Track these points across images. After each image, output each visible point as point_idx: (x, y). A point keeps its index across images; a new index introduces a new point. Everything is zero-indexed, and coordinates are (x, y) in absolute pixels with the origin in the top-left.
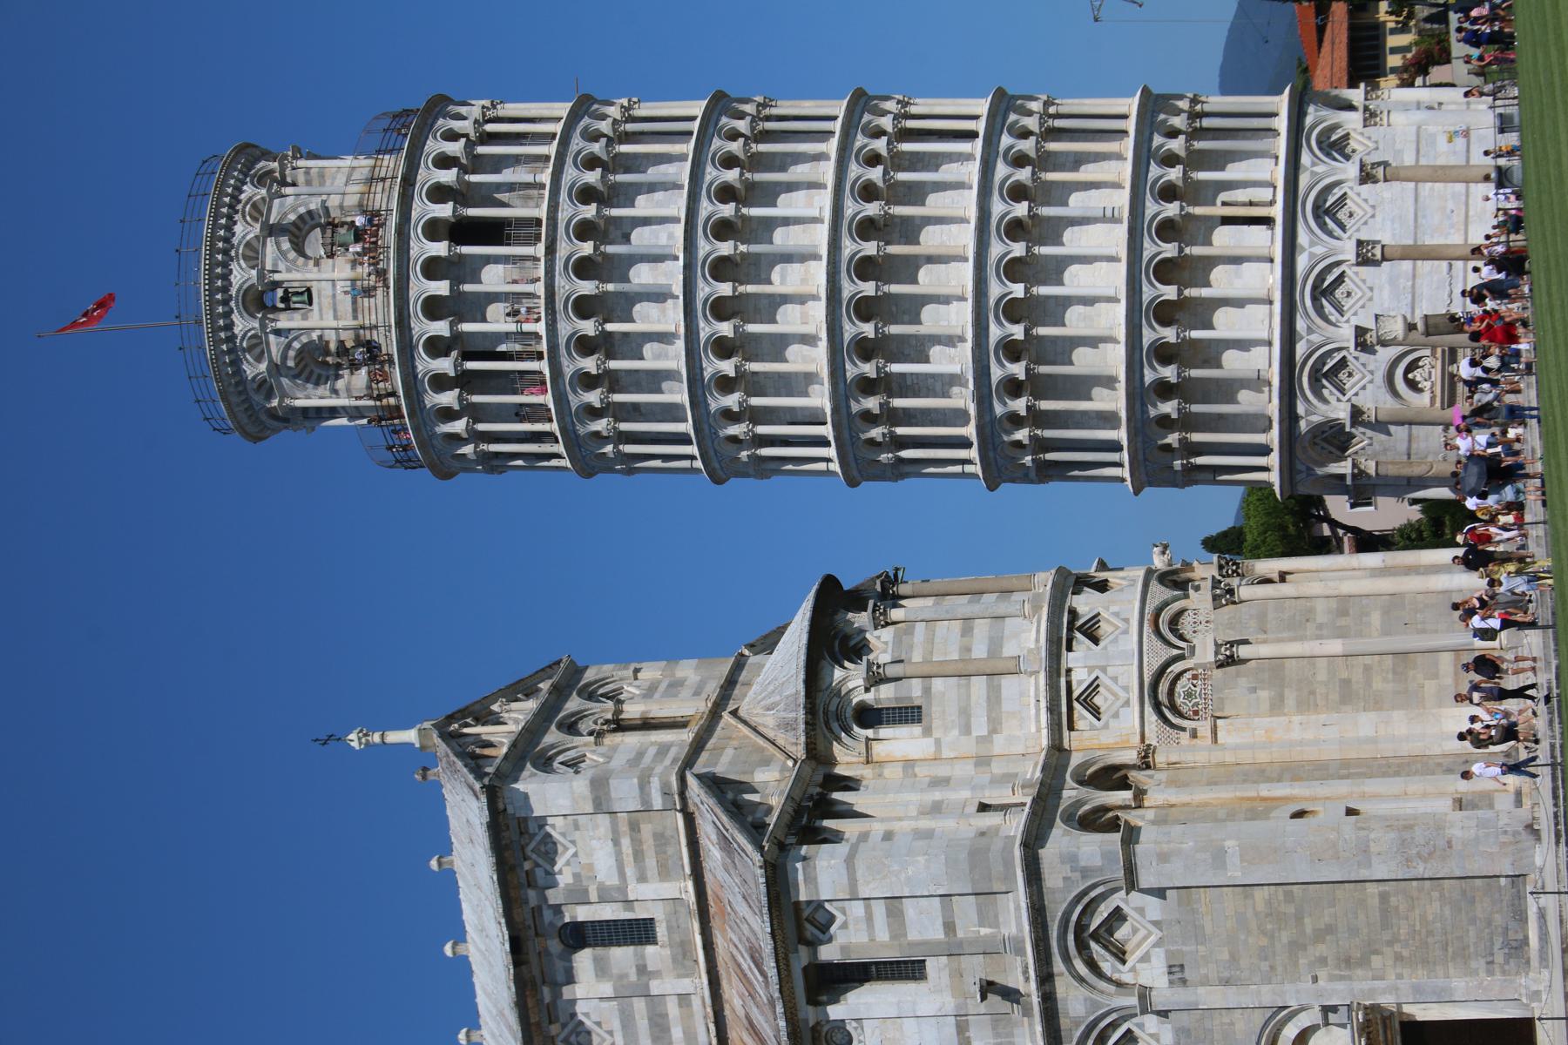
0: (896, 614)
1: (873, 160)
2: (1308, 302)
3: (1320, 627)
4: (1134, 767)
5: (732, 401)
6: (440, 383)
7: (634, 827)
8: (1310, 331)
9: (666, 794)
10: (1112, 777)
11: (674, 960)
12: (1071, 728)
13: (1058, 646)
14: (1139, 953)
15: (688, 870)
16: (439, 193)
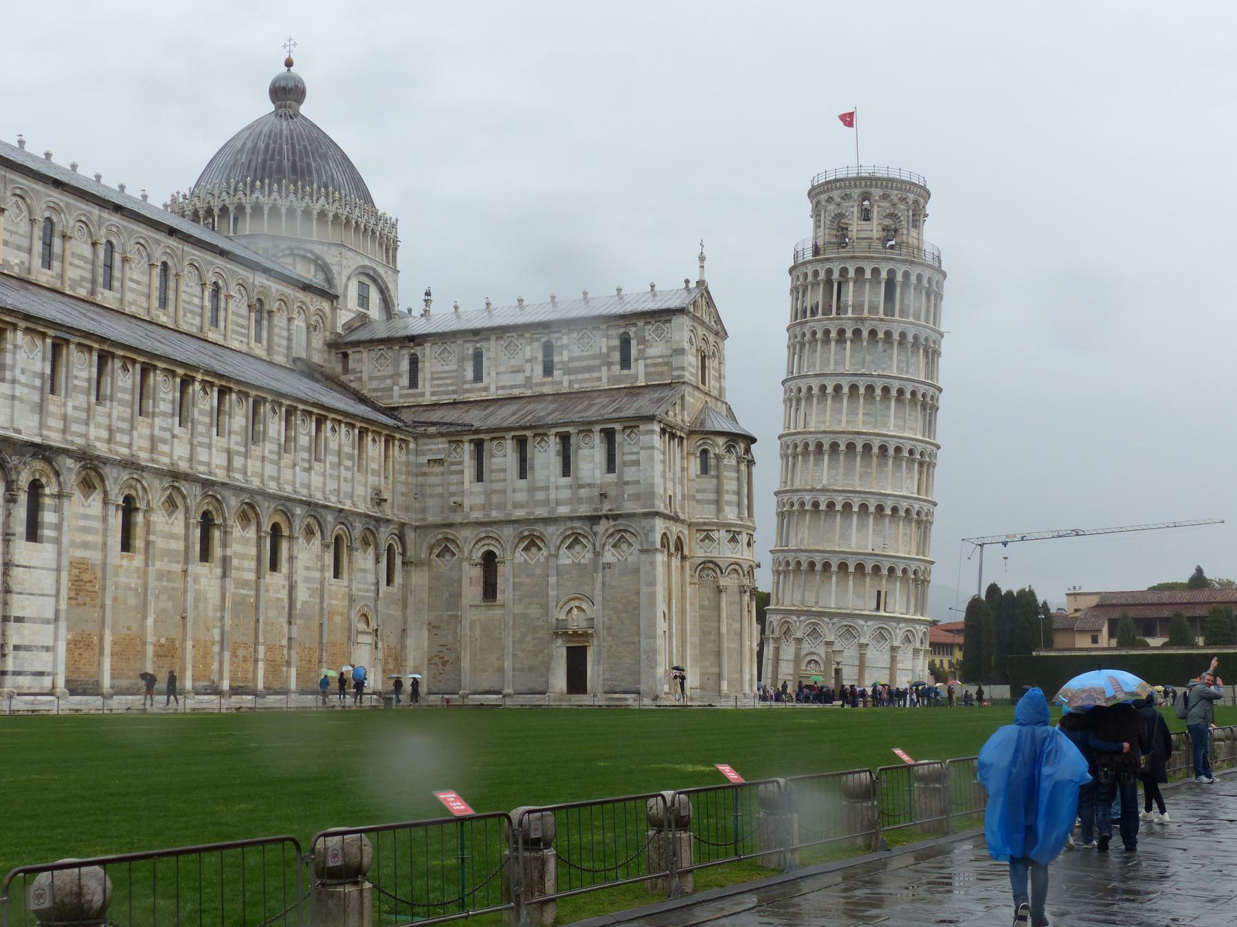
0: (743, 467)
2: (845, 623)
3: (731, 625)
4: (682, 554)
5: (815, 391)
6: (829, 272)
7: (666, 364)
8: (833, 624)
9: (679, 377)
10: (679, 545)
11: (615, 376)
12: (698, 530)
13: (728, 527)
14: (615, 553)
15: (649, 383)
16: (906, 275)
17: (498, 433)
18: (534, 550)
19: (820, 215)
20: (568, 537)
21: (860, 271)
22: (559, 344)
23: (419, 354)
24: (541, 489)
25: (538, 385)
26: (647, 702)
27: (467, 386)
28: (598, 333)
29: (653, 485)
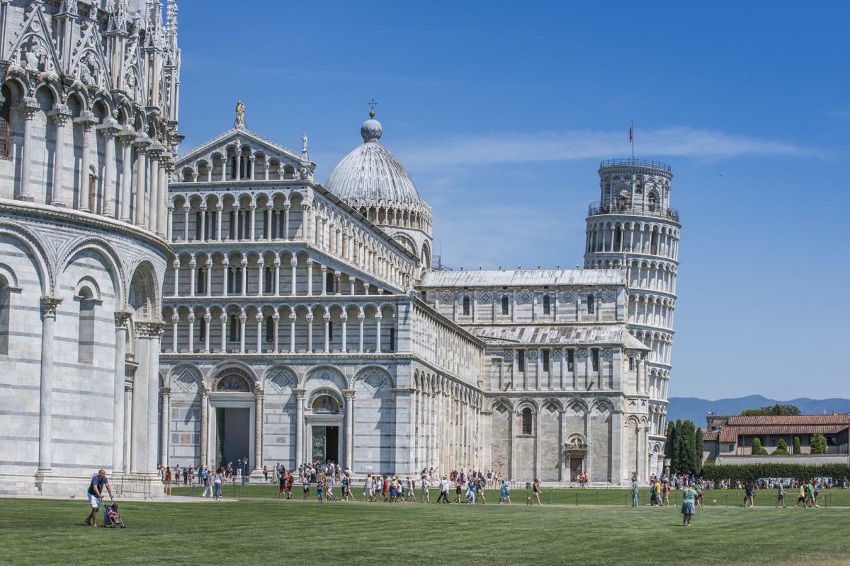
1: (663, 338)
9: (621, 320)
13: (641, 397)
16: (664, 229)
17: (533, 347)
18: (552, 408)
19: (609, 185)
20: (572, 403)
21: (637, 226)
22: (553, 296)
23: (470, 297)
24: (556, 377)
25: (540, 318)
26: (615, 486)
27: (498, 316)
28: (576, 293)
29: (619, 379)
